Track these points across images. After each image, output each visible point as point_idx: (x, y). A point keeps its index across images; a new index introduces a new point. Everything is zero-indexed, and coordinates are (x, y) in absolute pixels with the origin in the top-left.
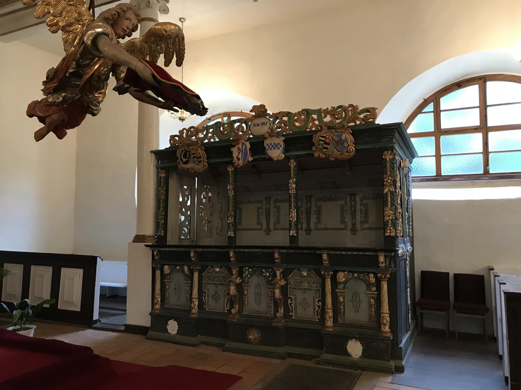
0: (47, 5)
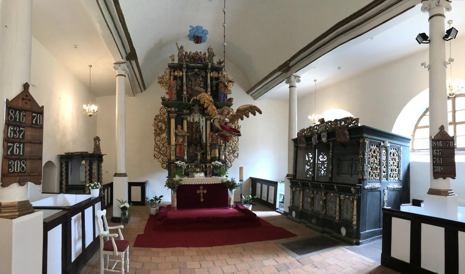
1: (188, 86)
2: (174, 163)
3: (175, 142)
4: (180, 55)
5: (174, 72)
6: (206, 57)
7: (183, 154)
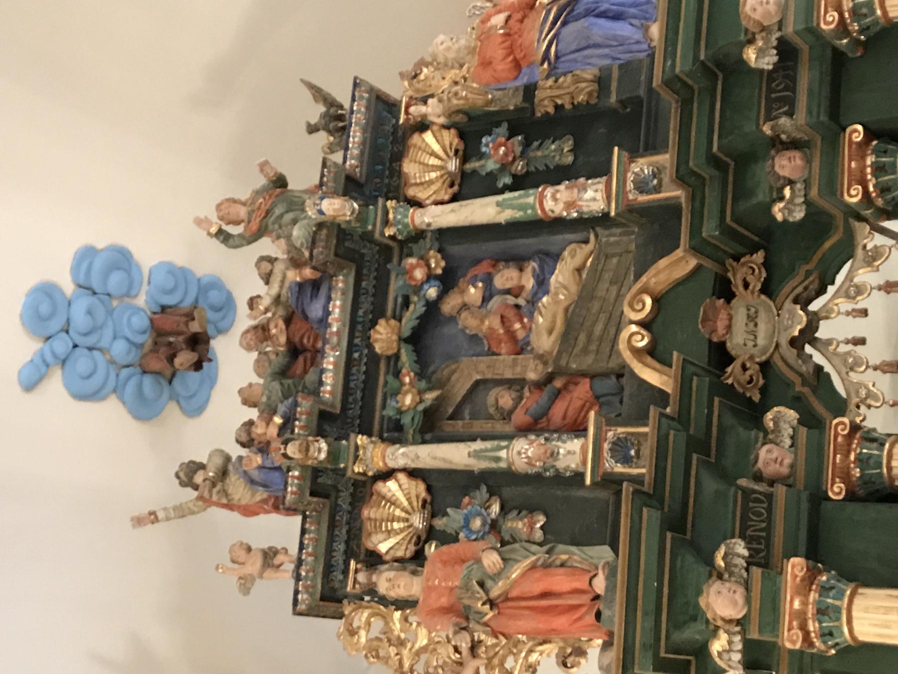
1: (520, 417)
4: (238, 489)
5: (373, 560)
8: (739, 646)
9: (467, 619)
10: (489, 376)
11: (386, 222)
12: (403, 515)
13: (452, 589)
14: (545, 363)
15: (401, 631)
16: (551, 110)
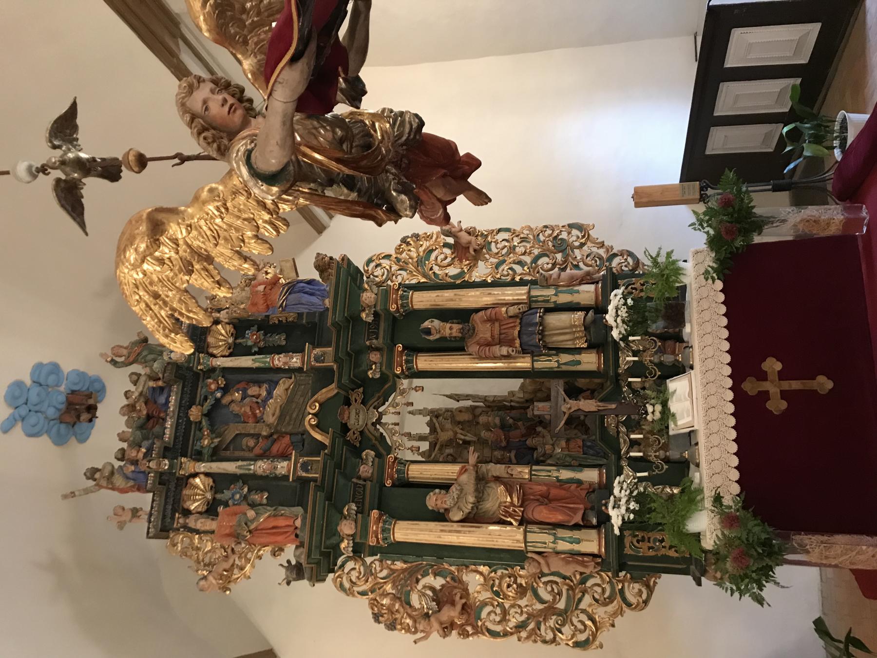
0: (243, 241)
1: (257, 450)
2: (621, 538)
3: (511, 524)
4: (119, 481)
5: (187, 513)
6: (145, 374)
7: (574, 486)
8: (352, 545)
9: (238, 538)
10: (243, 432)
11: (199, 363)
12: (201, 492)
13: (231, 526)
14: (270, 428)
15: (198, 543)
16: (277, 322)
